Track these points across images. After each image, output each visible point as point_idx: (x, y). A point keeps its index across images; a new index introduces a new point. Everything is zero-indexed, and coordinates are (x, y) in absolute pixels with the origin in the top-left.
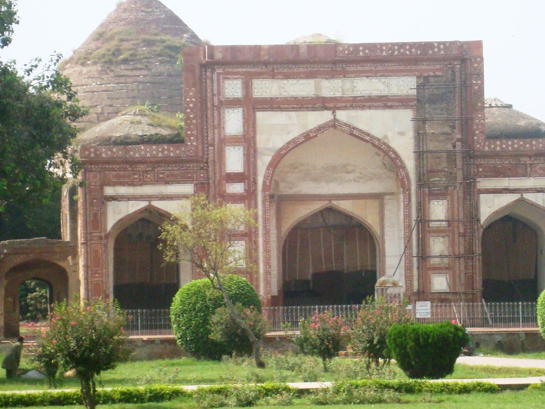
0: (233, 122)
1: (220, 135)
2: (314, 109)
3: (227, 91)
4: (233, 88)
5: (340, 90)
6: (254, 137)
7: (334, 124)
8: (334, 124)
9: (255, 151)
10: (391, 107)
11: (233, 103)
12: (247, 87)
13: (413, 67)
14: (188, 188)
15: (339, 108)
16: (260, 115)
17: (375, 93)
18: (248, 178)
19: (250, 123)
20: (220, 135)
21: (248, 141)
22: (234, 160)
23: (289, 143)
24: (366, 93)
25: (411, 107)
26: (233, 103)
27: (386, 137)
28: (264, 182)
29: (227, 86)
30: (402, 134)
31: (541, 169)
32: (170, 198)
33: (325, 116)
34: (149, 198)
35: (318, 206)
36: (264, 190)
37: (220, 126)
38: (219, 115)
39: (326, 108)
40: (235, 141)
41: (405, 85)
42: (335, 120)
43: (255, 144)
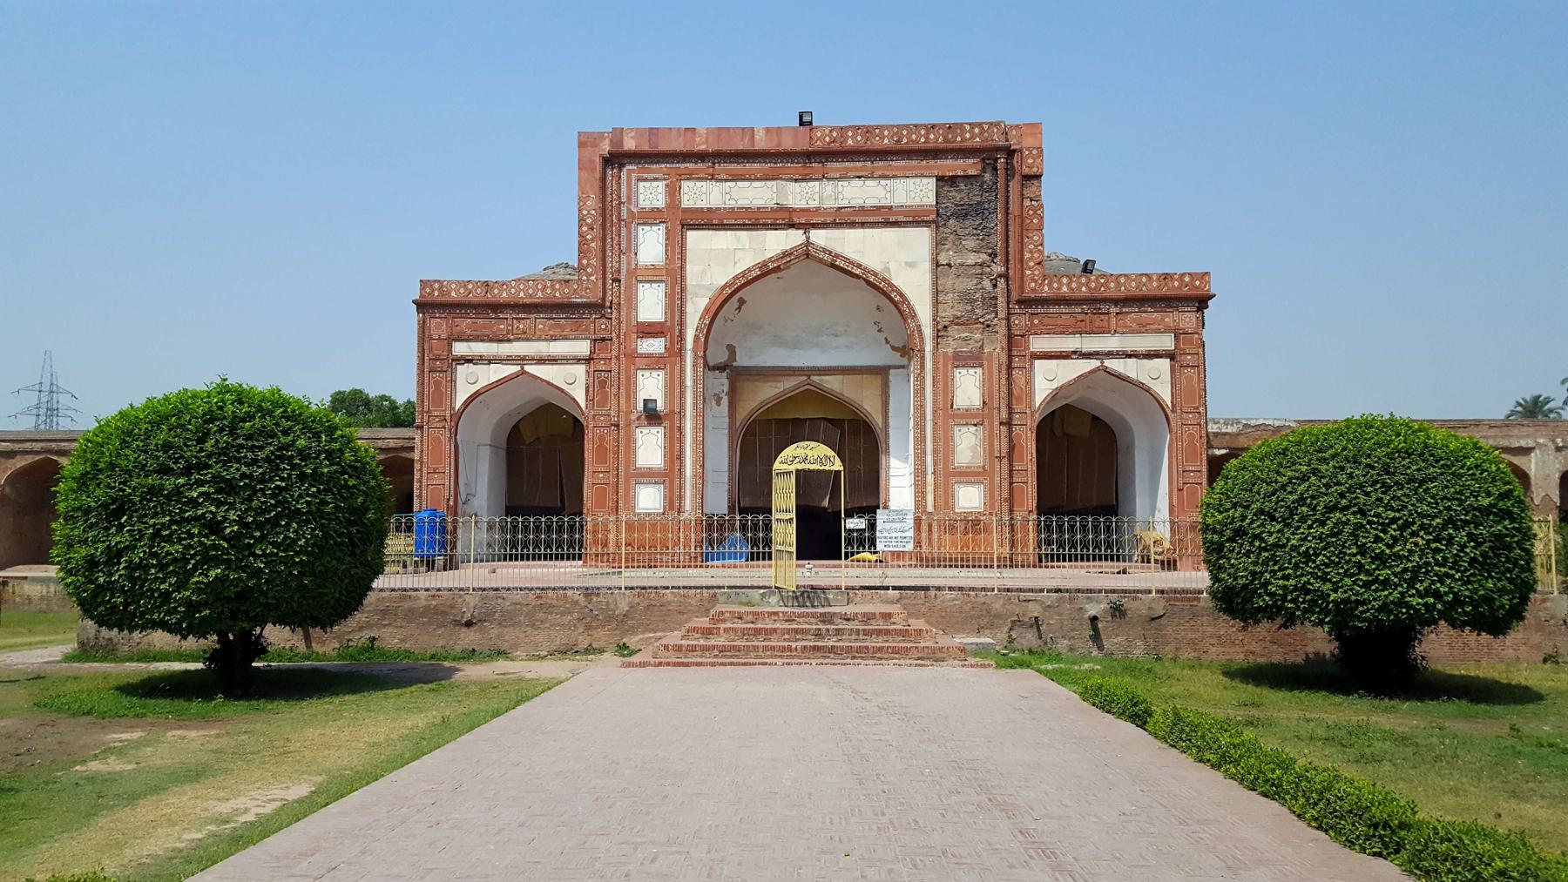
0: (650, 245)
1: (629, 264)
2: (775, 227)
3: (642, 197)
4: (651, 194)
5: (816, 197)
6: (682, 268)
7: (807, 252)
8: (807, 252)
9: (683, 290)
10: (896, 224)
11: (651, 217)
12: (673, 192)
13: (932, 162)
14: (582, 347)
15: (815, 226)
16: (690, 233)
17: (871, 202)
18: (671, 329)
19: (676, 250)
20: (629, 264)
21: (673, 275)
22: (650, 304)
23: (736, 278)
24: (857, 203)
25: (927, 224)
26: (651, 217)
27: (888, 269)
28: (696, 338)
29: (641, 190)
30: (911, 265)
31: (1133, 320)
32: (553, 360)
33: (794, 238)
34: (522, 360)
35: (790, 383)
36: (695, 350)
37: (631, 249)
38: (629, 232)
39: (792, 226)
40: (652, 275)
41: (918, 191)
42: (808, 243)
43: (683, 278)
